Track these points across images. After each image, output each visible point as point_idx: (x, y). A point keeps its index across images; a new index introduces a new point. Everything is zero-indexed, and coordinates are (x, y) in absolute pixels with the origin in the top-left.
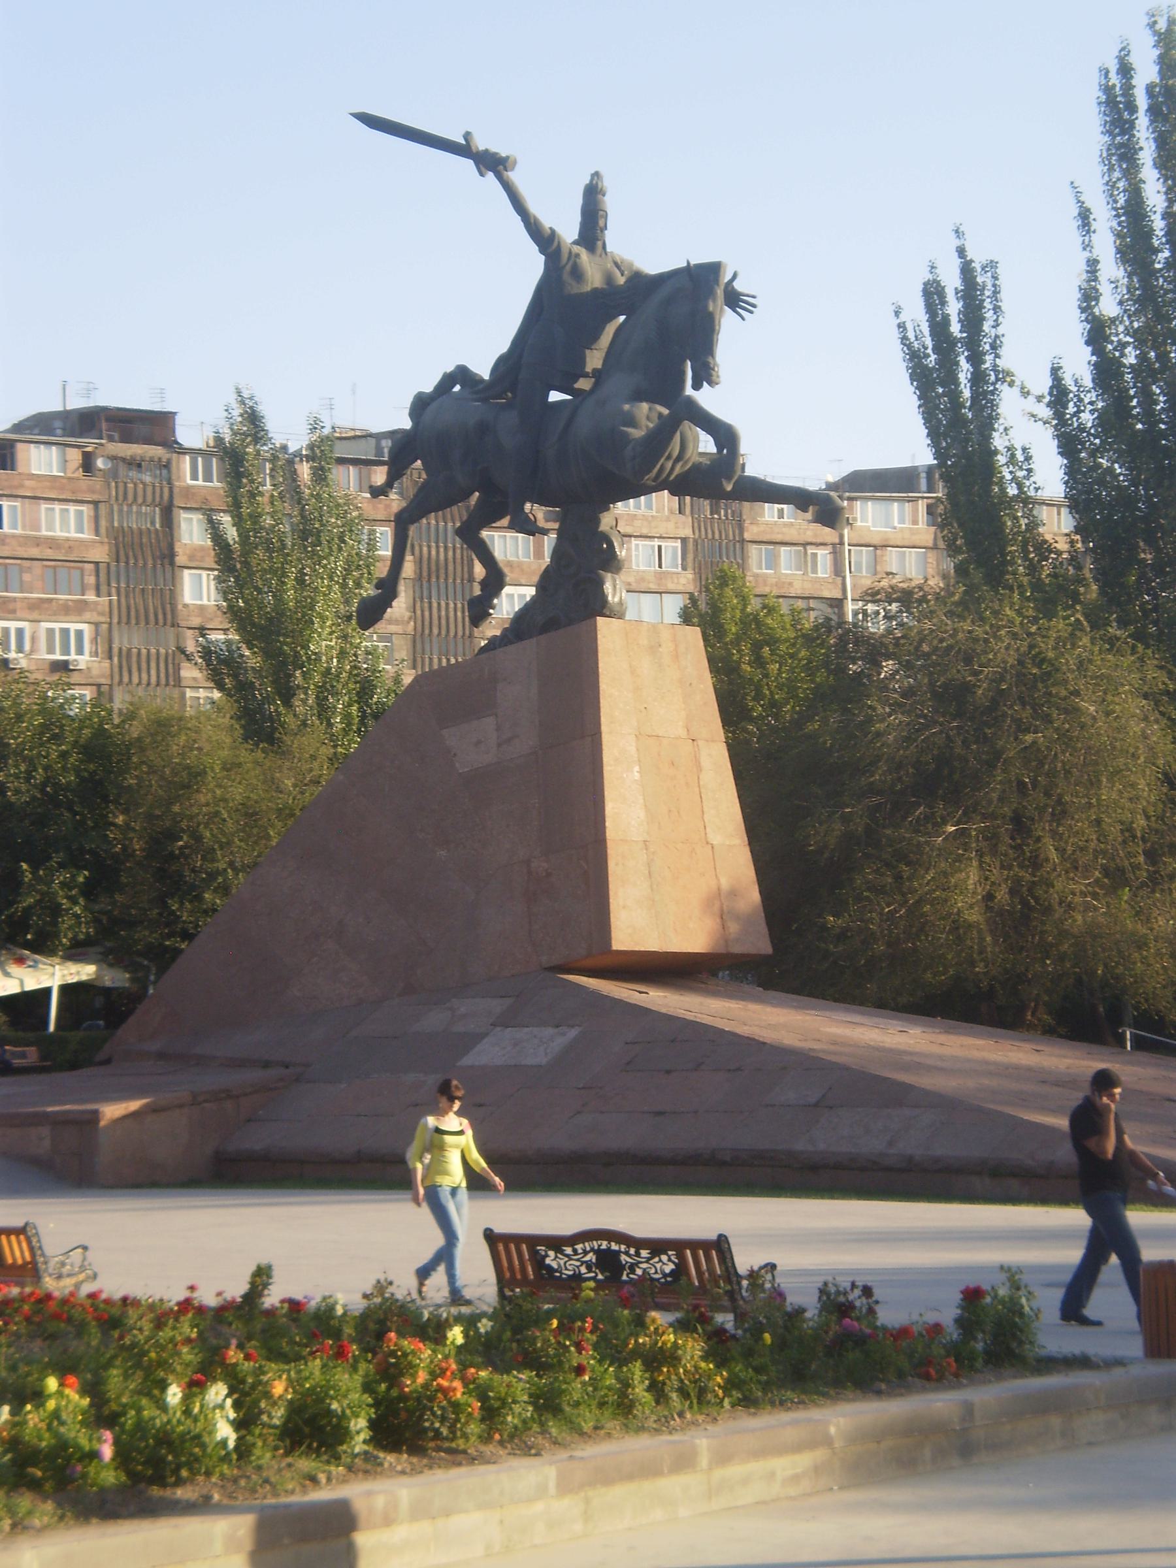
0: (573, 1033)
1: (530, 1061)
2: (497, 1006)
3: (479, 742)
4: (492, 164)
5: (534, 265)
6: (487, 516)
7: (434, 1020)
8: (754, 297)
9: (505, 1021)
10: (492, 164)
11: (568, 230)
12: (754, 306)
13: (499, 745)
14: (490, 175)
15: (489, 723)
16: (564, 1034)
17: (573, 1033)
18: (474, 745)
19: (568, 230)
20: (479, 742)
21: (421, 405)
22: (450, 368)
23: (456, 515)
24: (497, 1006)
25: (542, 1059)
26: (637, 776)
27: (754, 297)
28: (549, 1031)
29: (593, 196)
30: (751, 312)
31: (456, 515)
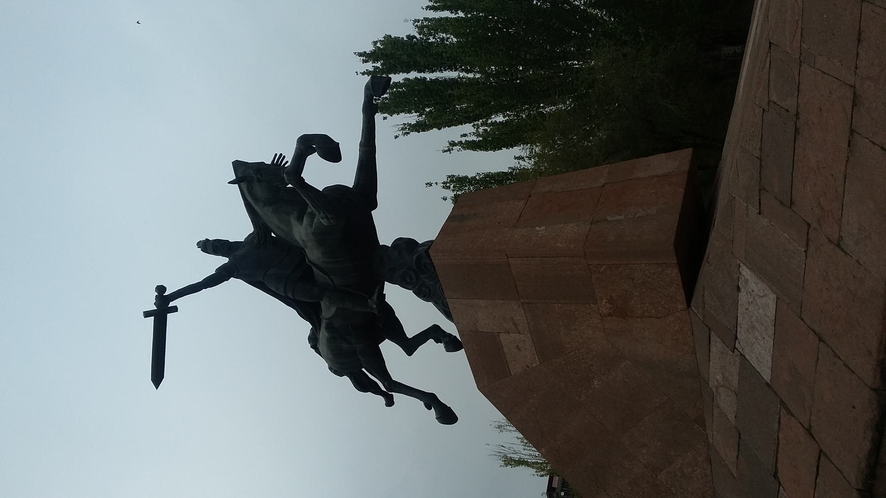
0: (746, 272)
1: (771, 312)
2: (717, 346)
3: (518, 347)
5: (235, 284)
7: (726, 402)
9: (731, 339)
13: (519, 333)
14: (171, 304)
16: (747, 281)
17: (746, 272)
18: (520, 351)
20: (518, 347)
21: (338, 370)
24: (717, 346)
25: (770, 300)
26: (540, 229)
28: (743, 297)
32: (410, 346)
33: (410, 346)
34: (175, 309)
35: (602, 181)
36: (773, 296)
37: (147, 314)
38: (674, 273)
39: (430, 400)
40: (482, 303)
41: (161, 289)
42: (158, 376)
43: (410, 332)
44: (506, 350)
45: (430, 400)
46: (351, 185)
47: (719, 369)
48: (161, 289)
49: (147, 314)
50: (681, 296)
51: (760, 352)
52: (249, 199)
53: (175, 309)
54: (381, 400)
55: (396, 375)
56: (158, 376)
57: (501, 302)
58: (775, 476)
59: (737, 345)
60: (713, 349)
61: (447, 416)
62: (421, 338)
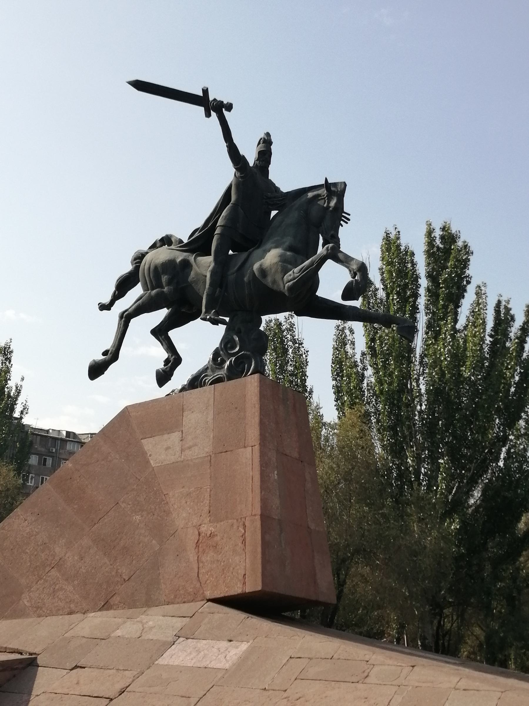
0: (244, 646)
2: (178, 623)
3: (168, 448)
4: (217, 108)
6: (176, 320)
8: (349, 215)
10: (217, 108)
11: (251, 158)
12: (349, 220)
13: (182, 450)
14: (213, 114)
15: (175, 436)
16: (237, 647)
17: (244, 646)
19: (251, 158)
20: (168, 448)
22: (164, 235)
23: (159, 315)
24: (178, 623)
25: (223, 664)
27: (349, 215)
29: (266, 142)
30: (347, 223)
31: (159, 315)
32: (160, 333)
33: (160, 333)
34: (208, 115)
35: (313, 526)
36: (227, 666)
37: (206, 91)
38: (236, 589)
39: (112, 355)
40: (211, 417)
41: (229, 107)
42: (140, 85)
43: (174, 334)
44: (166, 436)
45: (112, 355)
46: (320, 293)
47: (157, 622)
48: (229, 107)
49: (206, 91)
50: (218, 594)
51: (181, 656)
52: (310, 195)
53: (208, 115)
54: (107, 300)
55: (134, 322)
56: (140, 85)
57: (212, 436)
58: (76, 667)
59: (181, 639)
60: (175, 620)
61: (96, 370)
62: (170, 347)
